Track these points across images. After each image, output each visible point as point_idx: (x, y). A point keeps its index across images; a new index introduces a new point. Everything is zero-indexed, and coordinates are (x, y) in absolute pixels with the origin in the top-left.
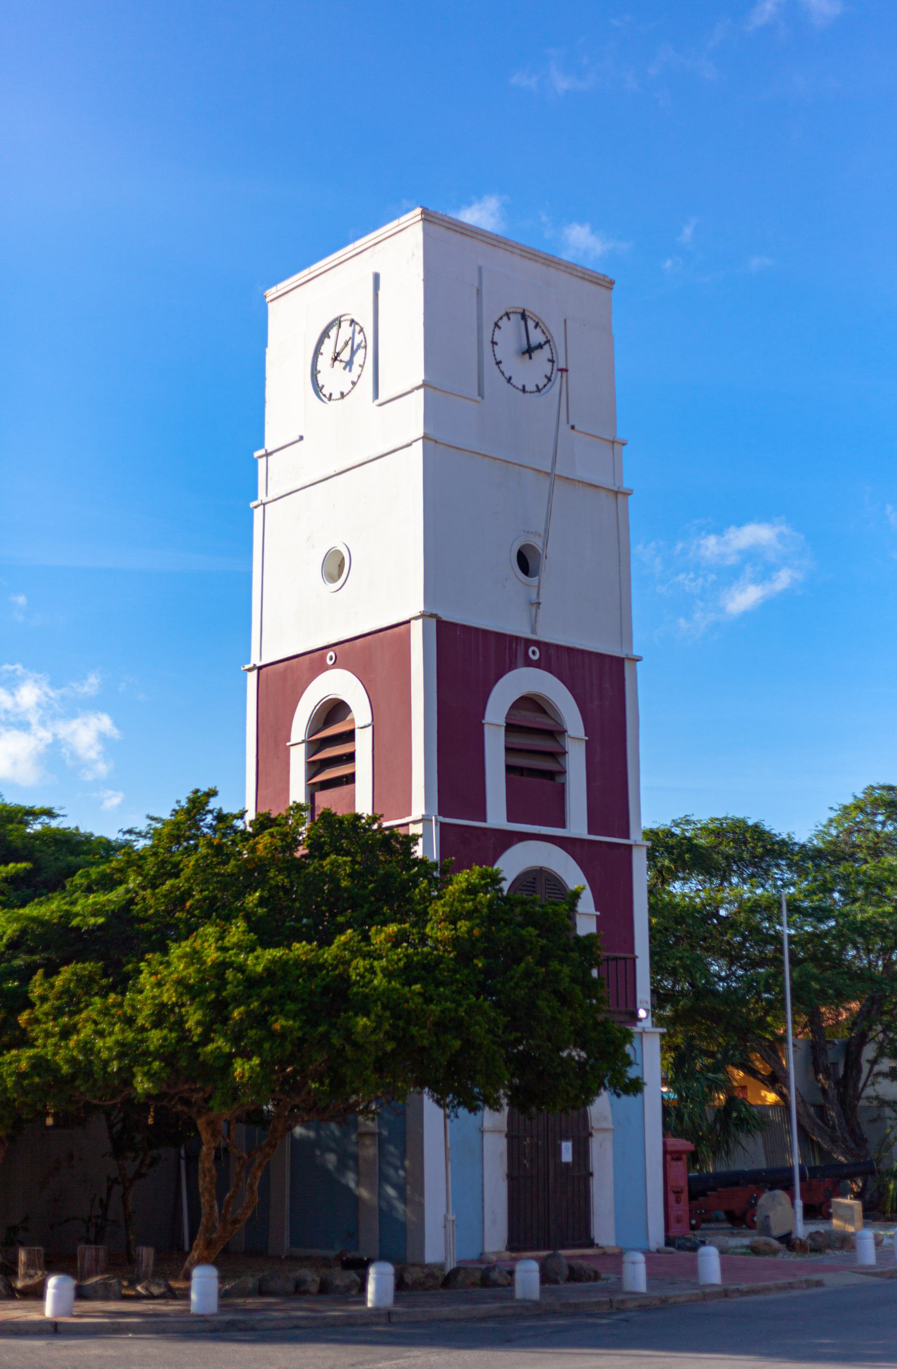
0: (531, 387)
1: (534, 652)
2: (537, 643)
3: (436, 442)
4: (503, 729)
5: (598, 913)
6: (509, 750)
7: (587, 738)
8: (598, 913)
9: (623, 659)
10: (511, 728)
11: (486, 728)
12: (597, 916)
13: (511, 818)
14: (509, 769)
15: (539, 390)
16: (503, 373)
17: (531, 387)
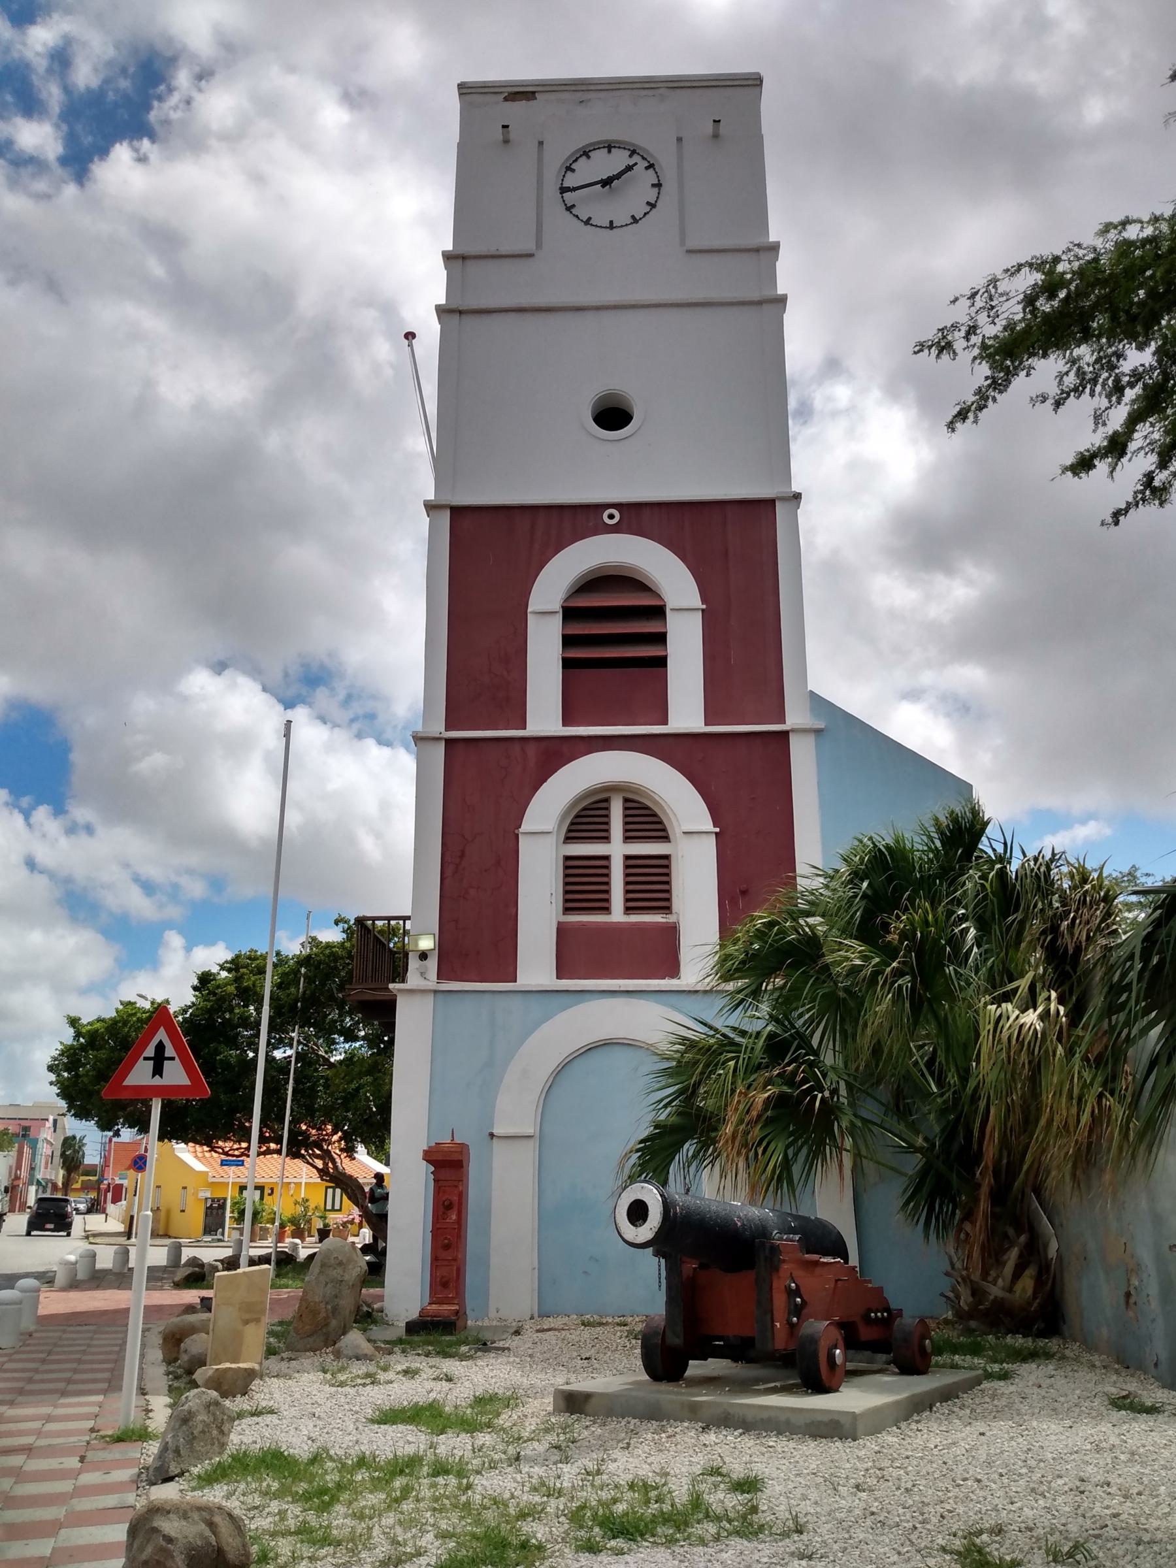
0: (622, 218)
1: (611, 517)
2: (618, 506)
3: (461, 312)
4: (558, 619)
5: (717, 830)
6: (568, 641)
7: (704, 607)
8: (717, 830)
9: (771, 503)
10: (570, 614)
11: (530, 617)
12: (716, 834)
13: (567, 721)
14: (568, 664)
15: (635, 220)
16: (577, 216)
17: (622, 218)
